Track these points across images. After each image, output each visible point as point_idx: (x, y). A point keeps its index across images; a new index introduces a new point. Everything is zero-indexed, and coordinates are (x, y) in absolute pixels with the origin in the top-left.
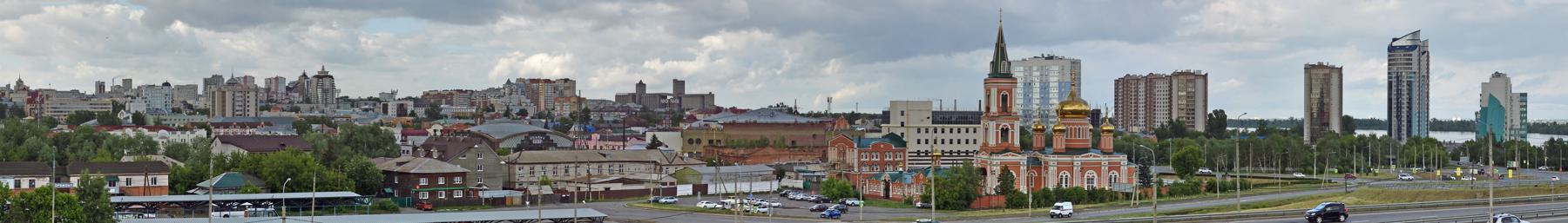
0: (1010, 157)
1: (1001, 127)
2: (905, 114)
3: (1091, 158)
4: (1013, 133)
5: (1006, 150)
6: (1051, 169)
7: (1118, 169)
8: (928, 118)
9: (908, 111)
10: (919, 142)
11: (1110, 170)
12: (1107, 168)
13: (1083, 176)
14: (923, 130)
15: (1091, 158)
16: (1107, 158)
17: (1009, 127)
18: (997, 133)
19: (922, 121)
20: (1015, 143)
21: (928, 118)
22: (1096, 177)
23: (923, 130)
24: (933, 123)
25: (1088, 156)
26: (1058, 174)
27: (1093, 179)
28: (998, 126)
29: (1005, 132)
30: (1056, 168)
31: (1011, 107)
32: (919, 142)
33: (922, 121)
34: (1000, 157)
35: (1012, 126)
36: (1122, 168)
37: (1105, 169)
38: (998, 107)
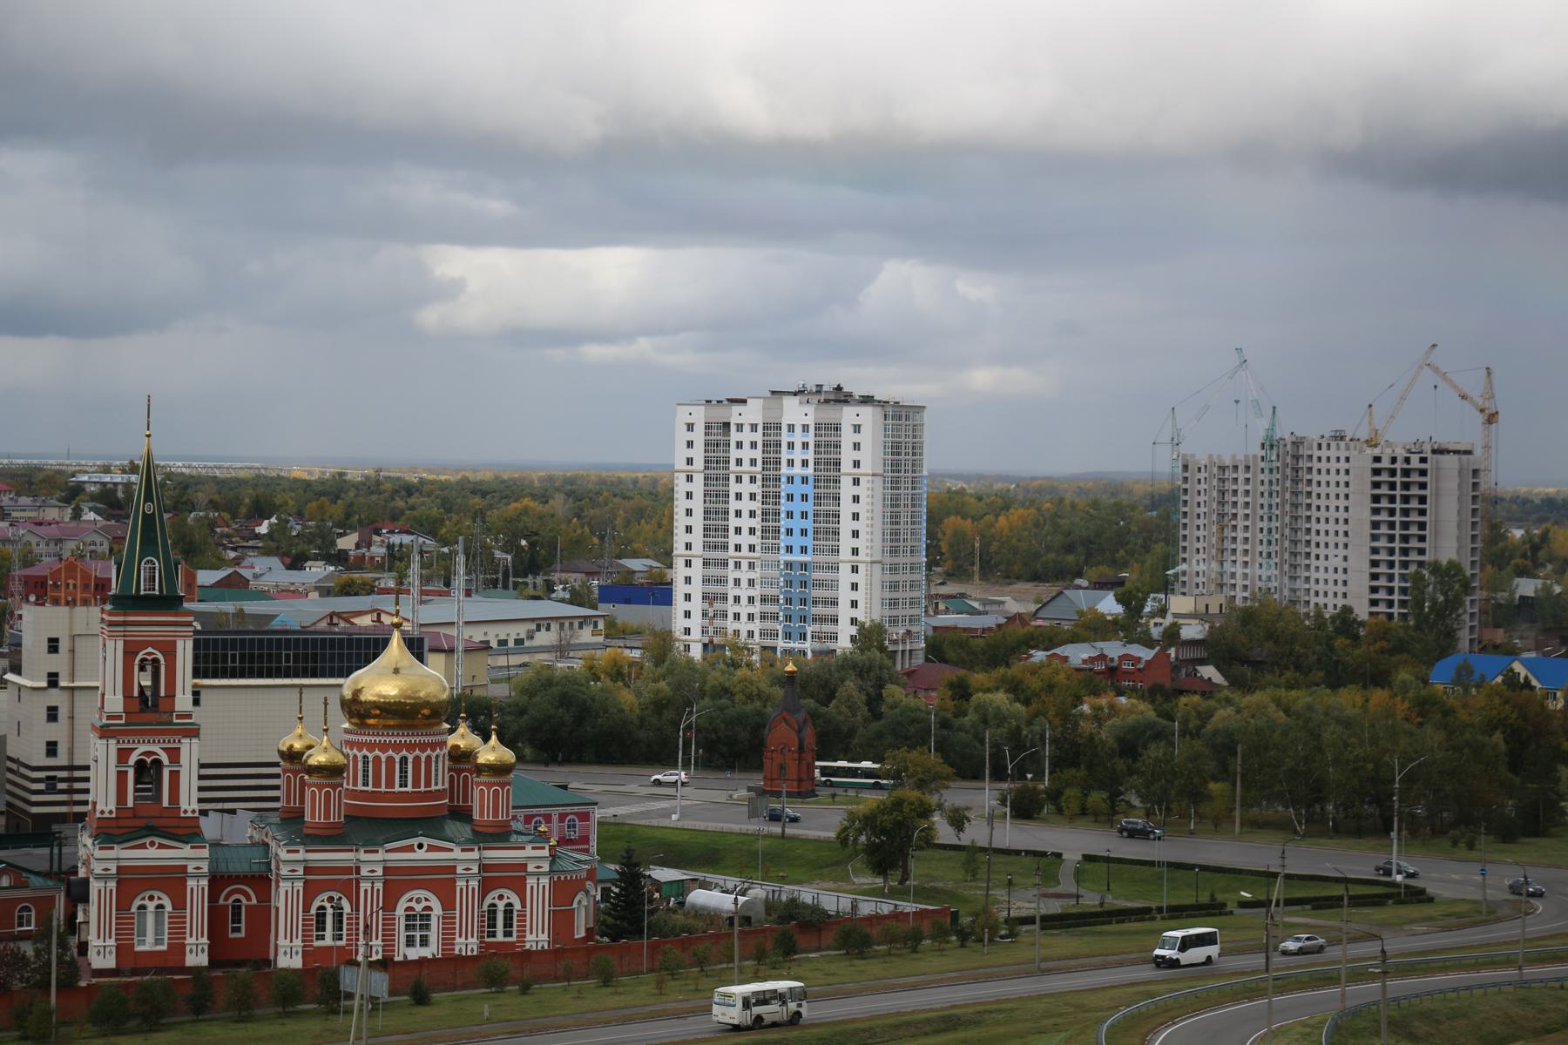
0: (152, 852)
2: (64, 646)
3: (421, 854)
4: (175, 776)
5: (152, 831)
6: (284, 886)
7: (519, 886)
9: (73, 638)
11: (486, 886)
12: (474, 884)
13: (389, 905)
15: (421, 854)
16: (475, 855)
18: (121, 776)
20: (184, 805)
22: (437, 910)
25: (410, 849)
26: (306, 909)
27: (428, 917)
28: (123, 755)
29: (147, 771)
30: (299, 885)
31: (171, 695)
34: (118, 852)
35: (174, 754)
36: (531, 881)
37: (467, 885)
38: (127, 695)
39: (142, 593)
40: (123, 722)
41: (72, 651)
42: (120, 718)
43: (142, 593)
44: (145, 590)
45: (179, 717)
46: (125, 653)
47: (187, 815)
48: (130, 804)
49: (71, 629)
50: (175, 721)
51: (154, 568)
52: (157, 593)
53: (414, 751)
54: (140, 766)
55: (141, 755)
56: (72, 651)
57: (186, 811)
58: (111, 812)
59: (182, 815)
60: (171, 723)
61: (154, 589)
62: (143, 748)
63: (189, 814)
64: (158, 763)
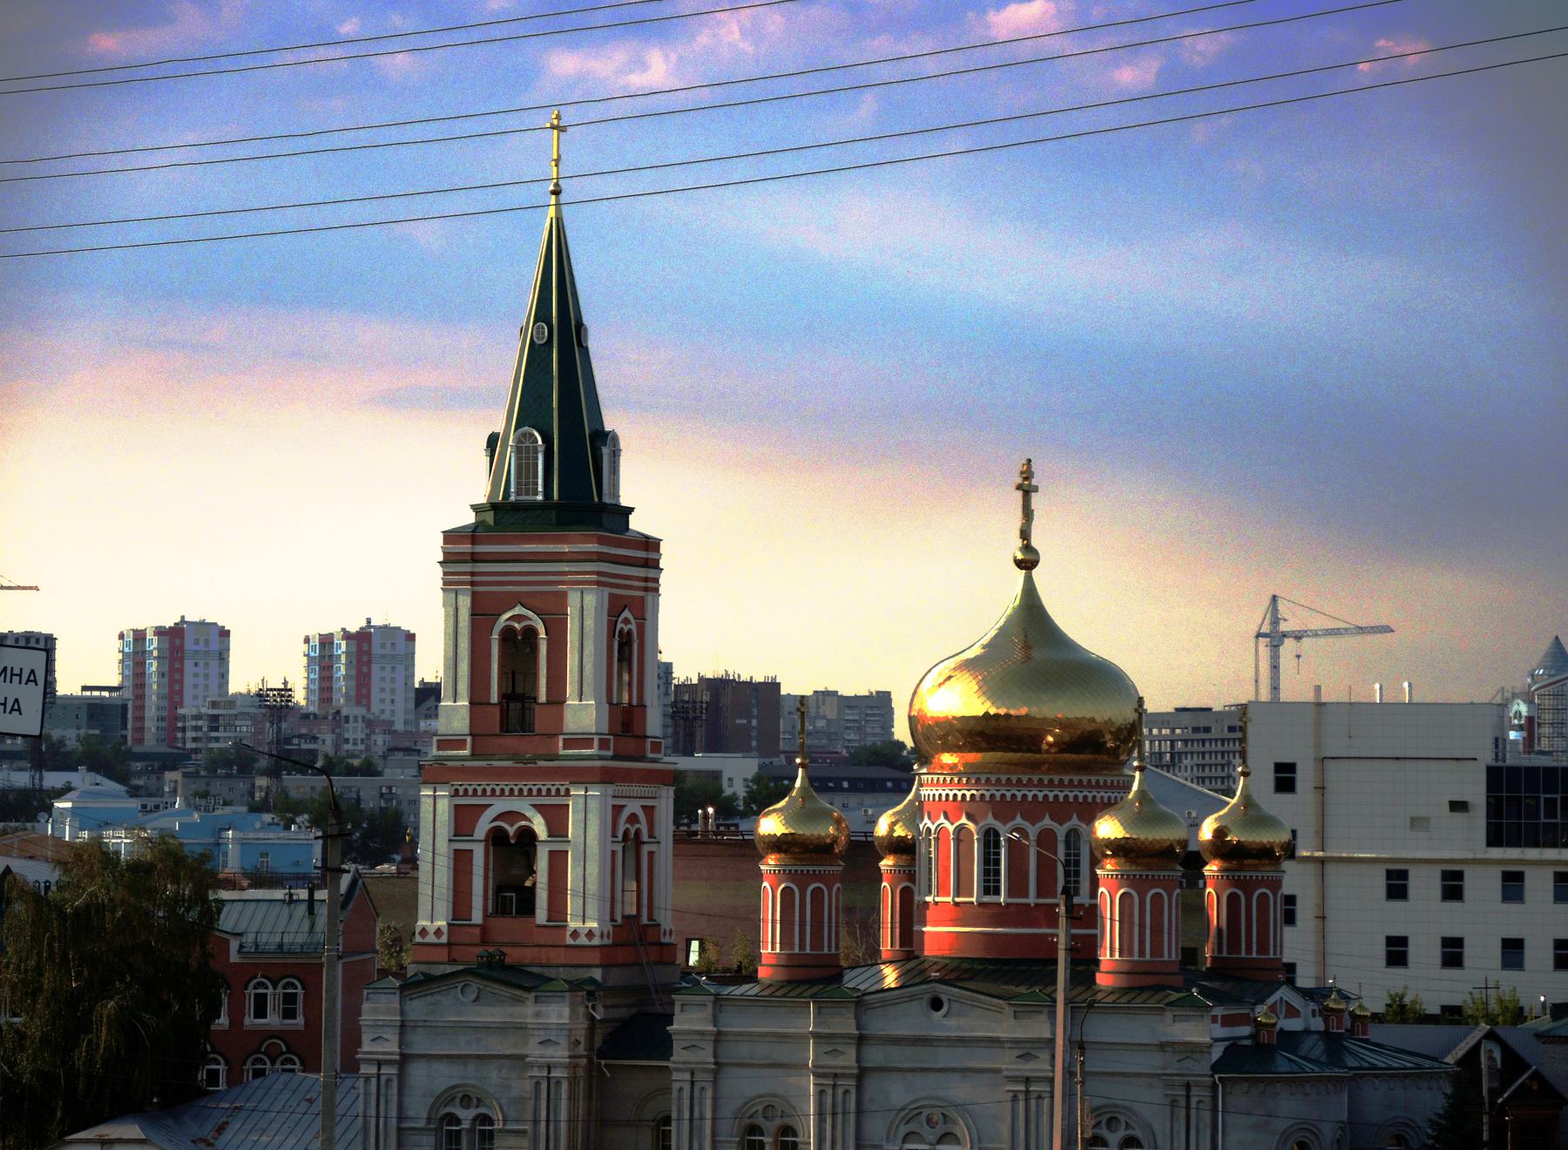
1: (483, 827)
8: (1458, 806)
10: (1397, 951)
14: (1424, 885)
17: (539, 826)
19: (1417, 823)
21: (1458, 806)
23: (1424, 885)
24: (1494, 840)
28: (463, 819)
31: (556, 699)
32: (1397, 951)
33: (1417, 823)
39: (513, 498)
40: (466, 752)
41: (1321, 789)
42: (460, 744)
43: (513, 498)
44: (518, 493)
45: (569, 744)
46: (474, 613)
47: (578, 942)
48: (477, 917)
49: (1318, 746)
50: (562, 752)
51: (536, 451)
52: (540, 498)
53: (1041, 818)
54: (497, 838)
55: (494, 820)
56: (1321, 789)
57: (575, 934)
58: (438, 932)
59: (570, 941)
60: (556, 757)
61: (536, 493)
62: (500, 805)
63: (583, 941)
64: (528, 836)
